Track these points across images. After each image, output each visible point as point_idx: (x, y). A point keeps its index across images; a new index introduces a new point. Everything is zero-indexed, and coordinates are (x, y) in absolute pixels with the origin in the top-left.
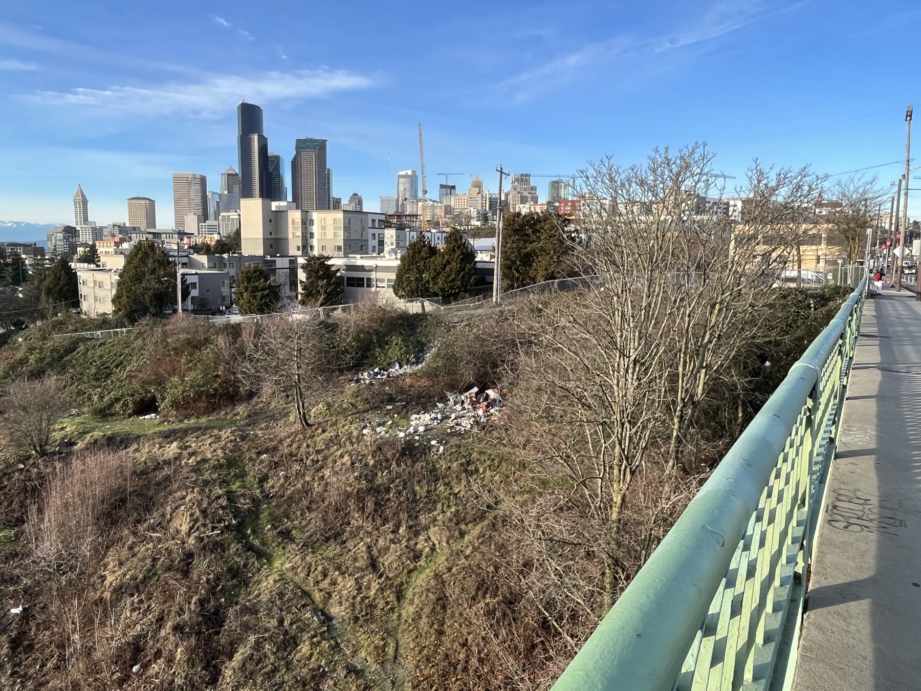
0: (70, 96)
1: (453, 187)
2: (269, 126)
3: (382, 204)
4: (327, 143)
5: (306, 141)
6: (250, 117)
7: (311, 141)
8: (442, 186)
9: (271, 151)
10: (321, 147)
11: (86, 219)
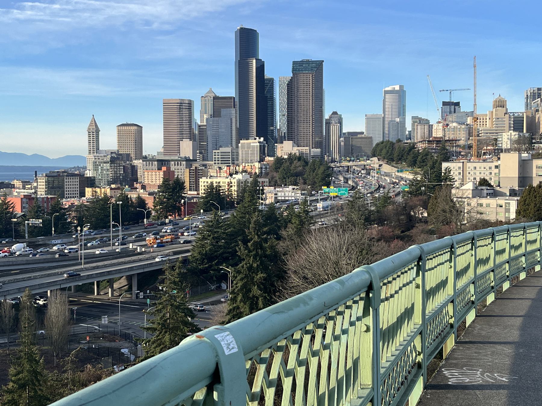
0: (15, 11)
1: (458, 104)
2: (265, 49)
3: (368, 124)
4: (323, 63)
5: (302, 63)
6: (247, 41)
7: (308, 62)
8: (445, 104)
9: (268, 75)
10: (315, 68)
11: (98, 149)
